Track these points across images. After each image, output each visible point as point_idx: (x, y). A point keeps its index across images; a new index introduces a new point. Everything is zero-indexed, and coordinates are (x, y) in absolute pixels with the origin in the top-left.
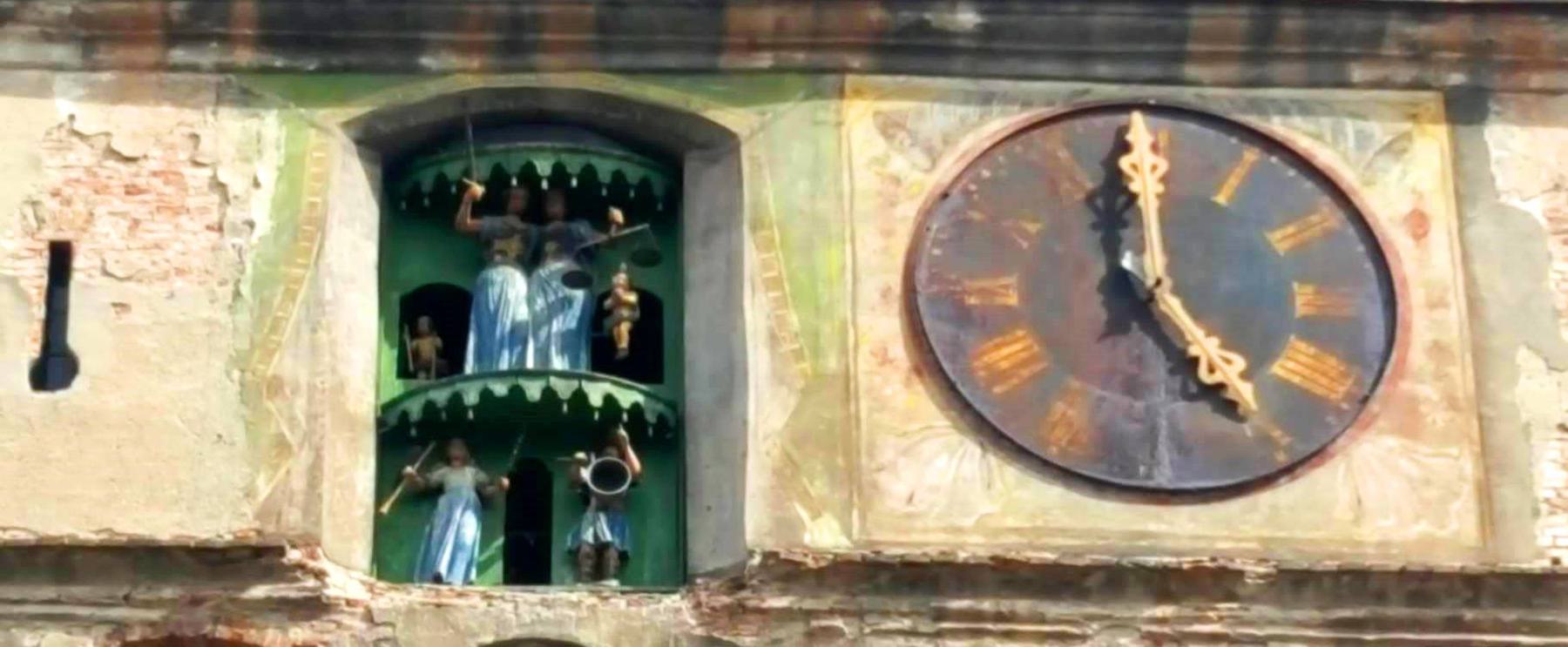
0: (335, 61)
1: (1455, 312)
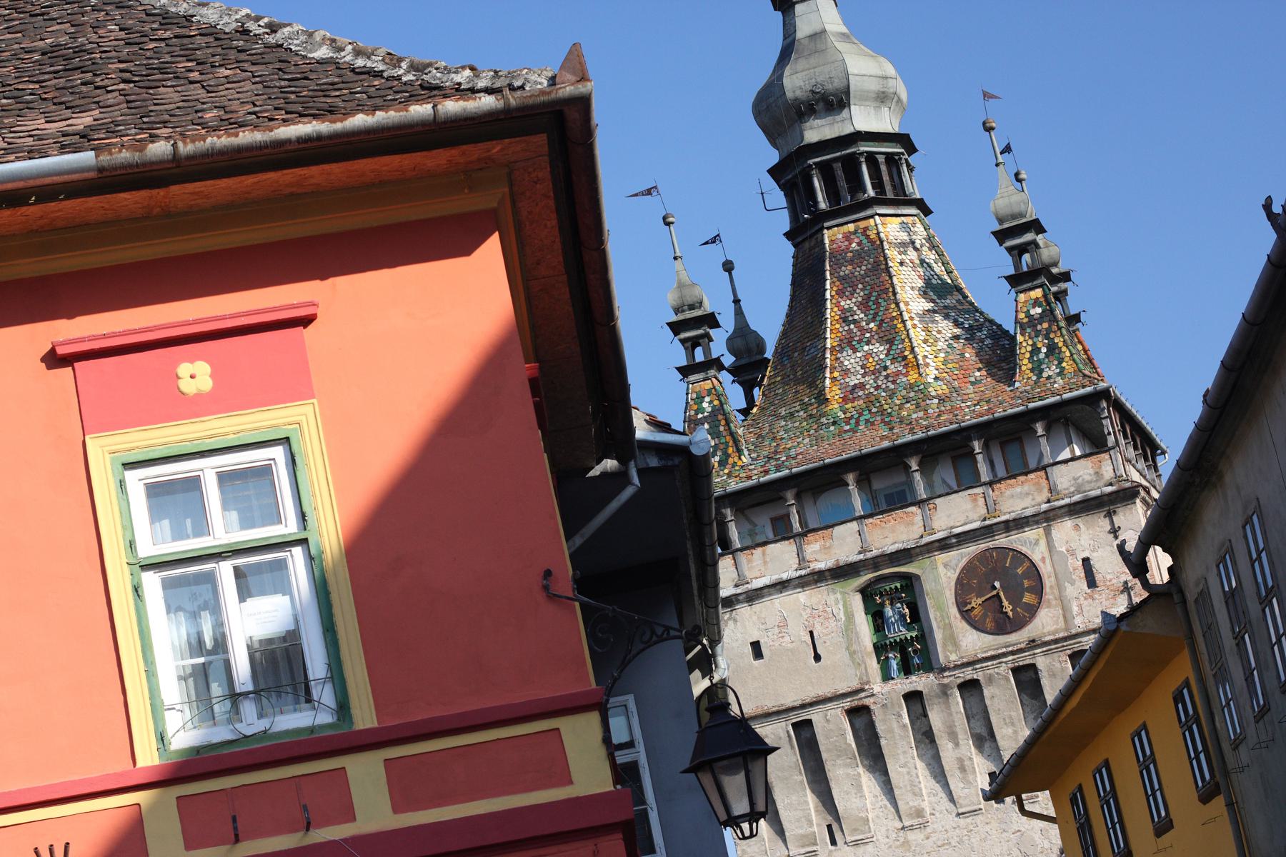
1: (1053, 579)
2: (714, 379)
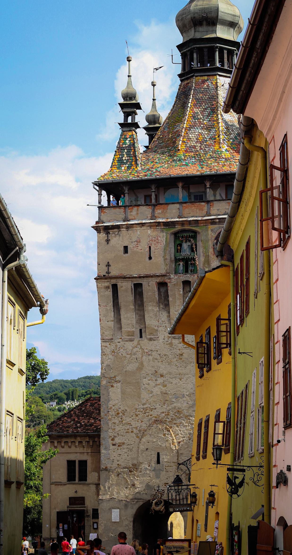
0: (169, 227)
2: (133, 132)
